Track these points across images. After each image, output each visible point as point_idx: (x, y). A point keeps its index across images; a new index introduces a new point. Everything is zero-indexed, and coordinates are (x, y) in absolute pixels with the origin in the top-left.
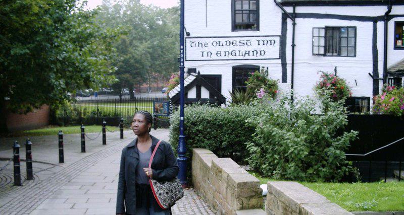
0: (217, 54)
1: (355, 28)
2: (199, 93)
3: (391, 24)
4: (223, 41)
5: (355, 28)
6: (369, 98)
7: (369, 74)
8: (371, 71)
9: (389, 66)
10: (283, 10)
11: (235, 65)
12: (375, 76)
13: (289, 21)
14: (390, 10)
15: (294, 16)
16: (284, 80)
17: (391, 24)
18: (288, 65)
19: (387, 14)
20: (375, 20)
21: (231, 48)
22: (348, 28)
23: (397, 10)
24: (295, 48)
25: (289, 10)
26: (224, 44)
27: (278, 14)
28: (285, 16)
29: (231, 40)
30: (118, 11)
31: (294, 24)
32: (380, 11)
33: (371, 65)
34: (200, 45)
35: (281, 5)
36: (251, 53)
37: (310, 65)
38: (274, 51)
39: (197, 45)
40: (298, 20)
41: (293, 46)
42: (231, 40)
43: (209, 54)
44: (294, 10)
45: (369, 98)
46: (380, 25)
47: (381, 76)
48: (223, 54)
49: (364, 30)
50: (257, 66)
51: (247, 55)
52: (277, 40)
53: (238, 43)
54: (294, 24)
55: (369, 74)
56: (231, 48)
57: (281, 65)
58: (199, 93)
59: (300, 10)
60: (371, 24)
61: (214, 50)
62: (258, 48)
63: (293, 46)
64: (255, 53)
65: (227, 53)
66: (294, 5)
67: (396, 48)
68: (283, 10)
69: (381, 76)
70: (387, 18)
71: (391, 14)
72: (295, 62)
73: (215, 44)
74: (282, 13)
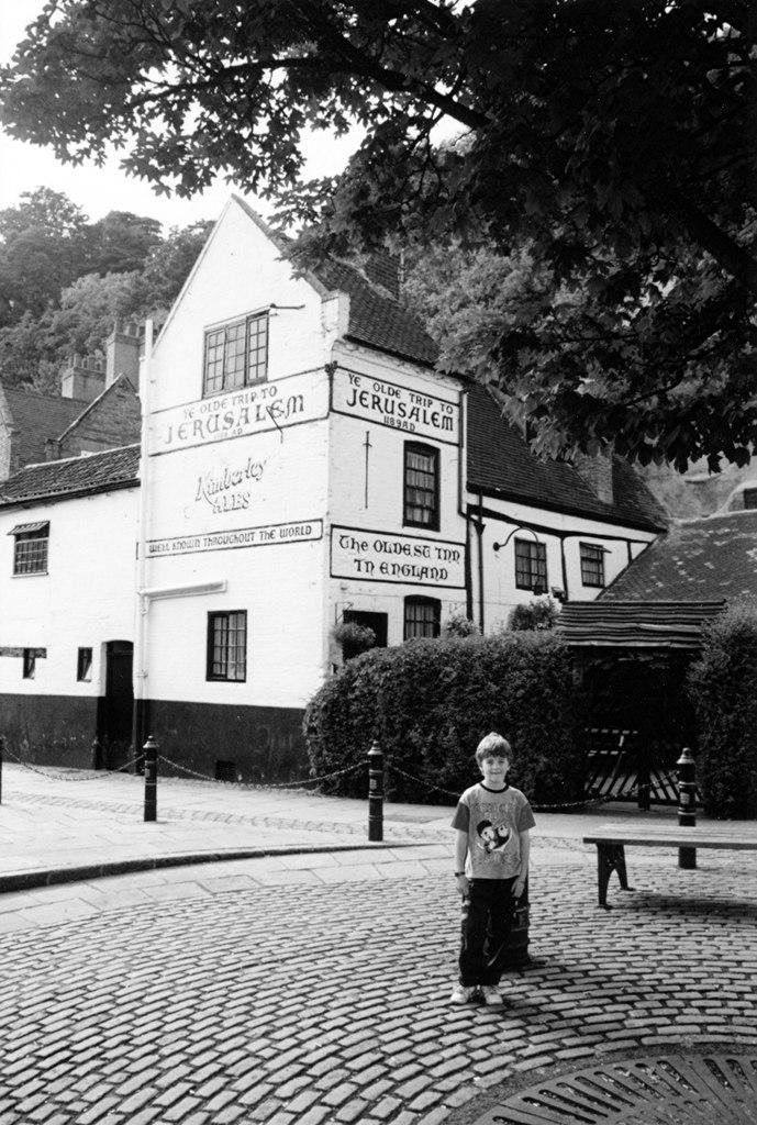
0: (381, 568)
4: (391, 540)
20: (562, 535)
21: (402, 559)
26: (393, 548)
29: (403, 541)
34: (356, 546)
36: (429, 573)
38: (456, 574)
39: (350, 545)
42: (403, 541)
43: (370, 565)
44: (481, 501)
48: (390, 569)
51: (424, 575)
52: (462, 550)
53: (412, 551)
56: (402, 559)
61: (378, 558)
62: (440, 564)
64: (435, 572)
65: (397, 568)
73: (378, 545)
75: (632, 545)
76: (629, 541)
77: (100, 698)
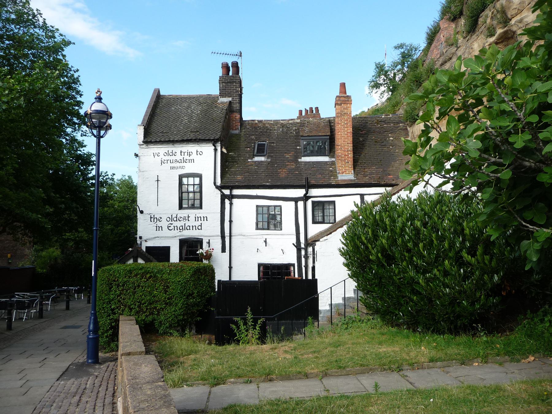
3: (309, 203)
5: (280, 206)
6: (294, 264)
7: (293, 244)
8: (294, 241)
9: (309, 236)
10: (222, 192)
11: (181, 238)
13: (227, 202)
14: (307, 193)
15: (231, 197)
16: (223, 250)
17: (309, 203)
18: (226, 238)
19: (305, 195)
20: (296, 200)
22: (275, 206)
23: (314, 192)
25: (227, 192)
27: (218, 194)
28: (223, 197)
31: (231, 204)
32: (300, 193)
33: (295, 237)
35: (220, 188)
37: (244, 237)
40: (235, 201)
41: (231, 221)
44: (231, 192)
45: (294, 264)
47: (303, 246)
49: (288, 208)
50: (200, 239)
54: (231, 204)
55: (293, 244)
57: (220, 238)
59: (236, 192)
63: (231, 221)
66: (231, 188)
67: (314, 222)
68: (222, 192)
69: (303, 246)
70: (306, 198)
71: (308, 195)
72: (233, 234)
75: (365, 196)
76: (362, 196)
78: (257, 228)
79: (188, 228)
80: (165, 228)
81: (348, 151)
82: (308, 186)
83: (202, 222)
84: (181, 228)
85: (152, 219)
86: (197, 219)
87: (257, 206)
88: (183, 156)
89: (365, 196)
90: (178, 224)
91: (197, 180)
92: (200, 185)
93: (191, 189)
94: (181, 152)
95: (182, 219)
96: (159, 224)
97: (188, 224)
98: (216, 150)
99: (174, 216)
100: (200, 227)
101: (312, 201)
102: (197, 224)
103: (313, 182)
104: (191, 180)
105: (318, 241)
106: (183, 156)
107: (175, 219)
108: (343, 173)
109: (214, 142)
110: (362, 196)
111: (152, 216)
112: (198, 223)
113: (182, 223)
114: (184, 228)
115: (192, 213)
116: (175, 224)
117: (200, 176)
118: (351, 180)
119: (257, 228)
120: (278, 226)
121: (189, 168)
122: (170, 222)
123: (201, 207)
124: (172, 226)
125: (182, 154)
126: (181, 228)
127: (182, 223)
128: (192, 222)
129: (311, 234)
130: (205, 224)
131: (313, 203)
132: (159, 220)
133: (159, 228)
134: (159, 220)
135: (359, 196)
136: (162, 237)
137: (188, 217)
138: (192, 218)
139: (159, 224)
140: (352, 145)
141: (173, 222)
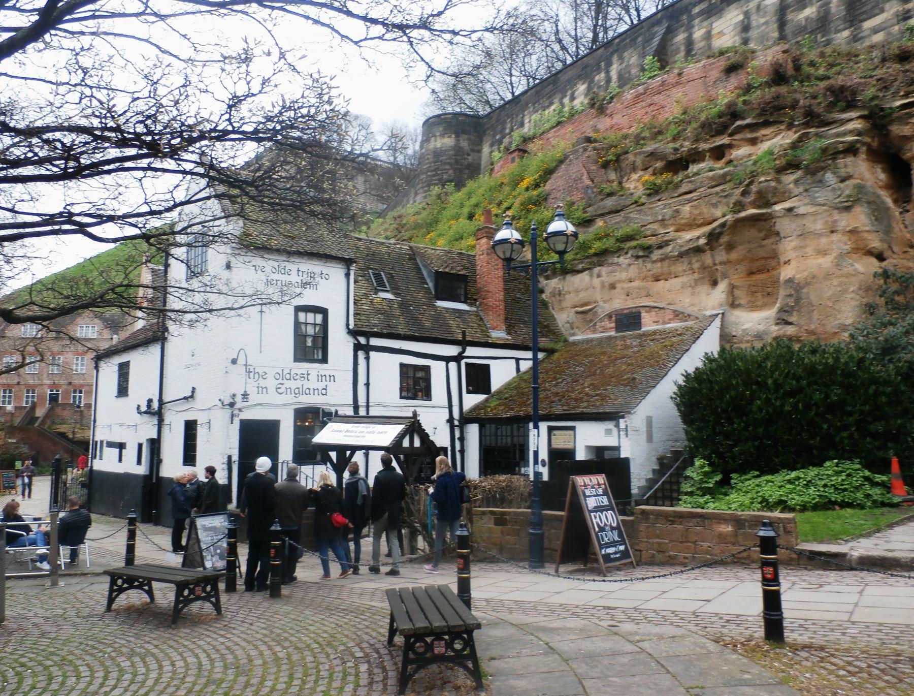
1: (427, 369)
2: (412, 441)
8: (447, 417)
12: (450, 420)
13: (361, 355)
14: (464, 351)
15: (367, 349)
20: (448, 359)
23: (471, 351)
24: (371, 387)
25: (362, 340)
27: (350, 342)
28: (358, 347)
30: (837, 359)
31: (367, 358)
32: (453, 350)
33: (447, 410)
35: (353, 333)
40: (372, 354)
41: (367, 385)
44: (368, 341)
46: (453, 365)
47: (456, 423)
49: (437, 370)
54: (367, 358)
58: (412, 441)
59: (374, 342)
60: (444, 363)
63: (367, 385)
66: (368, 335)
67: (469, 392)
69: (456, 423)
70: (457, 359)
74: (355, 344)
75: (521, 362)
76: (518, 360)
77: (145, 477)
78: (401, 397)
79: (307, 392)
80: (272, 390)
81: (499, 301)
82: (464, 343)
83: (328, 383)
84: (297, 391)
85: (252, 375)
86: (321, 377)
87: (403, 366)
88: (301, 278)
89: (521, 362)
90: (293, 384)
91: (319, 318)
92: (325, 325)
93: (310, 330)
94: (298, 271)
95: (298, 377)
96: (262, 383)
97: (307, 385)
98: (347, 275)
99: (286, 371)
100: (324, 392)
101: (467, 364)
102: (321, 385)
103: (468, 338)
104: (310, 317)
105: (629, 413)
106: (301, 278)
107: (288, 376)
108: (494, 329)
109: (347, 262)
110: (518, 360)
111: (252, 370)
112: (322, 385)
113: (298, 383)
114: (298, 392)
115: (315, 368)
116: (288, 384)
117: (324, 312)
118: (500, 339)
119: (401, 397)
120: (427, 394)
121: (310, 298)
122: (280, 381)
123: (324, 360)
124: (283, 387)
125: (300, 273)
126: (297, 391)
127: (298, 383)
128: (313, 383)
129: (467, 406)
130: (331, 385)
131: (467, 364)
132: (264, 376)
133: (262, 390)
134: (264, 376)
135: (514, 361)
136: (268, 405)
137: (308, 374)
138: (313, 376)
139: (262, 383)
140: (502, 293)
141: (285, 381)
